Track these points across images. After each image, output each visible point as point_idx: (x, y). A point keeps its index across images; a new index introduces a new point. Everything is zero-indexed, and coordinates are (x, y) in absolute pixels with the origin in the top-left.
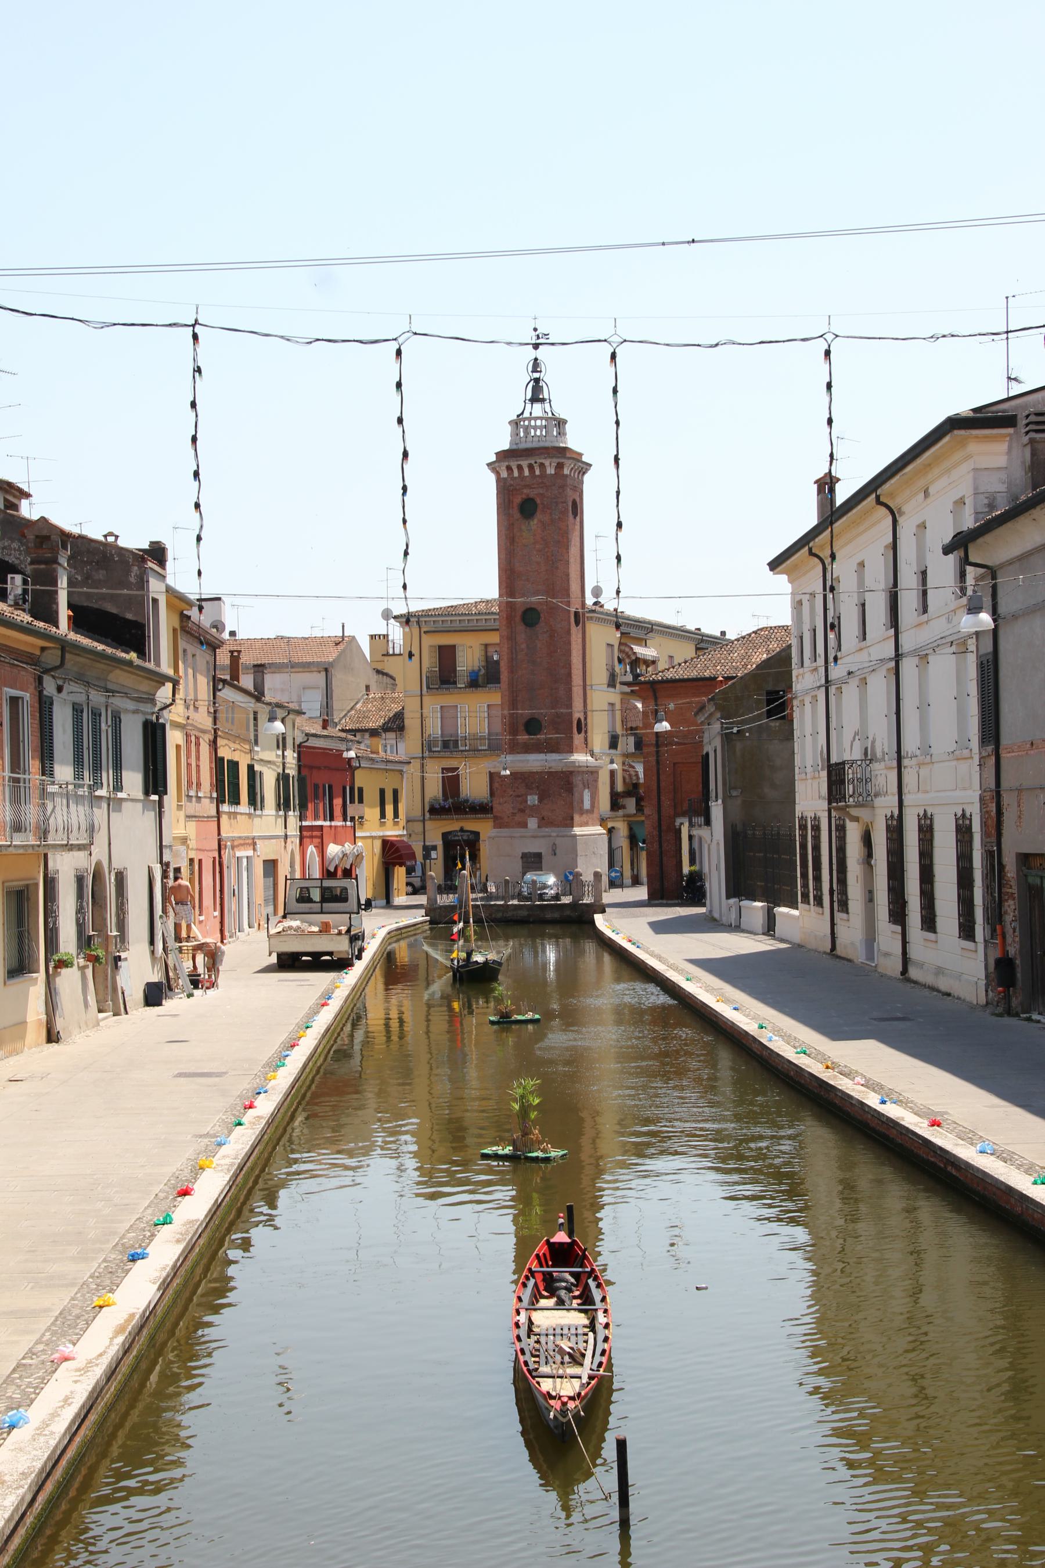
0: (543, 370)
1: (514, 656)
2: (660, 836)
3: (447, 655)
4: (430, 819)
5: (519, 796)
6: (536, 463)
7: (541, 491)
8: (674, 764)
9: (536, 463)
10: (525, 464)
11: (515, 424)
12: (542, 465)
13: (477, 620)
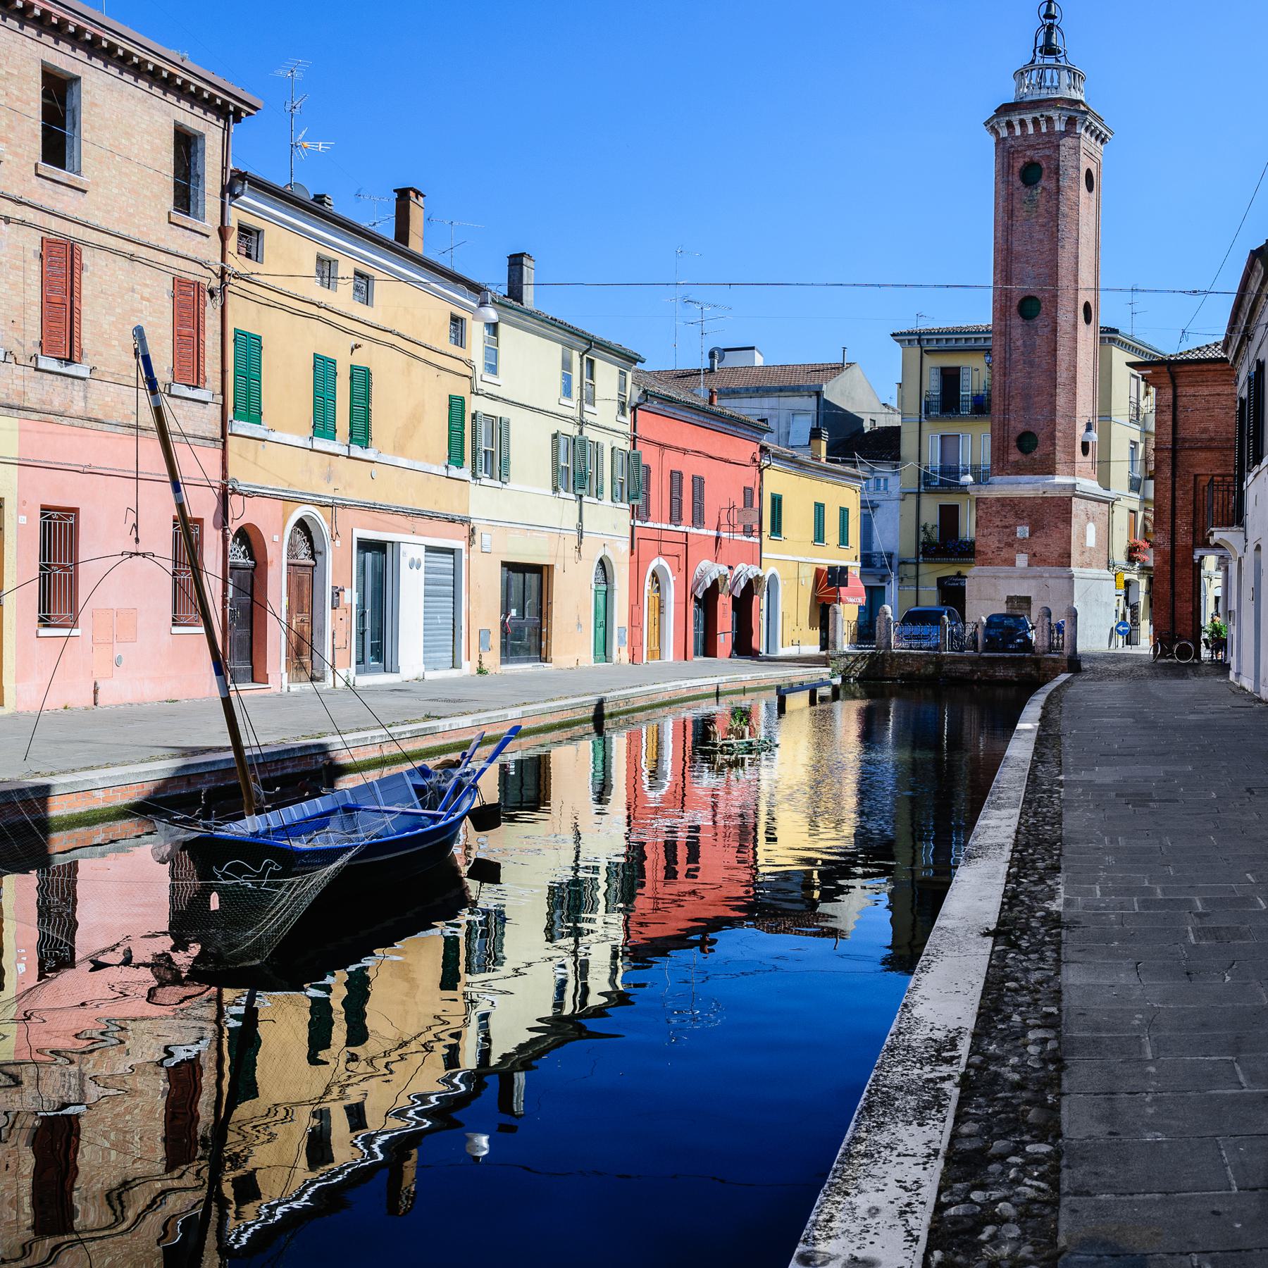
0: (1059, 17)
1: (1008, 356)
2: (1173, 572)
3: (950, 378)
4: (925, 562)
5: (1006, 527)
6: (1042, 116)
7: (1047, 152)
8: (1196, 476)
9: (1042, 116)
10: (1028, 118)
11: (1020, 74)
12: (1049, 120)
13: (985, 339)
